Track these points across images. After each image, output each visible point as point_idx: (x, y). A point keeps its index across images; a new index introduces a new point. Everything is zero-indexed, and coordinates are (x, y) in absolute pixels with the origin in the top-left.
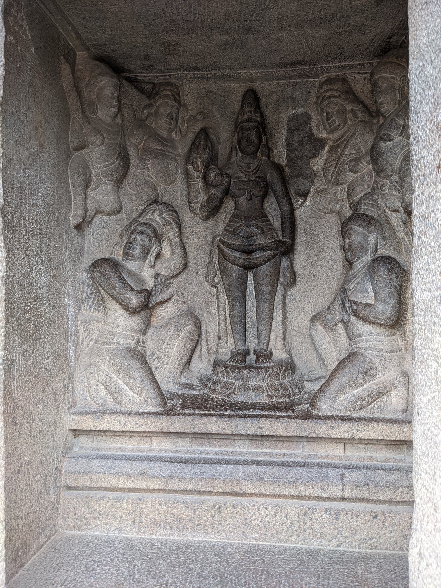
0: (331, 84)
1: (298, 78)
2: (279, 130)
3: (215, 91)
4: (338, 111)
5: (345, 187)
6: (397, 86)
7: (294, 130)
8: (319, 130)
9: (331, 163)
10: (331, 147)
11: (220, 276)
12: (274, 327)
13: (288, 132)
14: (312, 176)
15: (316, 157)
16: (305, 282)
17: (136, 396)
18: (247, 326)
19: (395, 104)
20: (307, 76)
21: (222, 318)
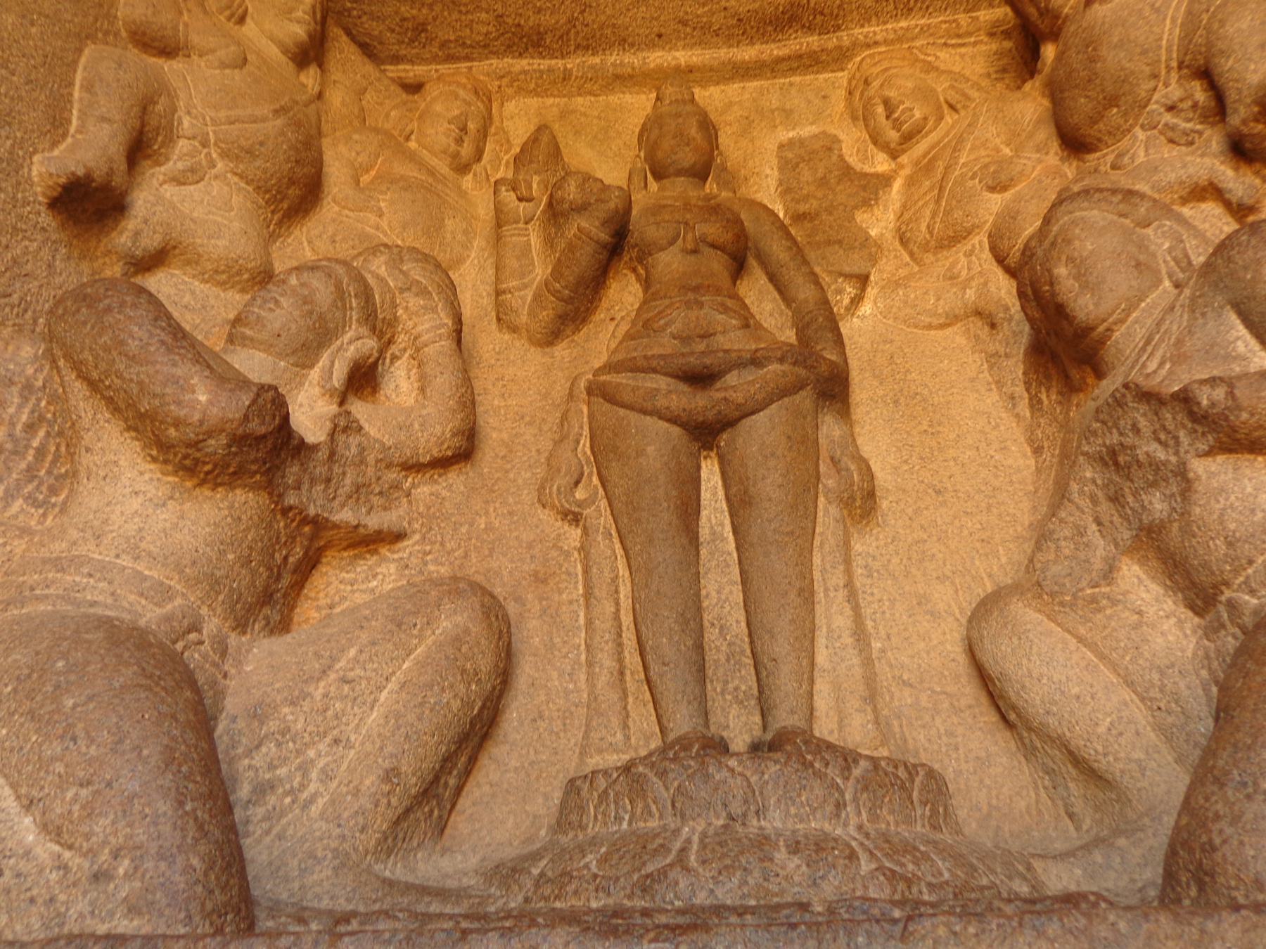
1: (793, 71)
3: (583, 109)
5: (980, 240)
8: (865, 159)
9: (920, 203)
11: (595, 480)
12: (821, 658)
13: (781, 169)
16: (910, 511)
17: (46, 850)
18: (710, 656)
21: (604, 625)
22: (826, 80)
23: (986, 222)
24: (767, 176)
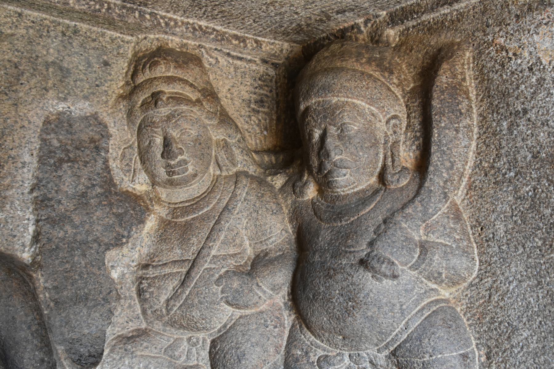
0: (178, 66)
1: (82, 20)
2: (13, 153)
4: (197, 141)
5: (205, 338)
6: (380, 136)
7: (61, 161)
9: (167, 270)
10: (165, 225)
13: (41, 160)
14: (108, 296)
15: (122, 244)
19: (372, 175)
20: (111, 24)
22: (113, 40)
23: (213, 329)
24: (24, 163)
